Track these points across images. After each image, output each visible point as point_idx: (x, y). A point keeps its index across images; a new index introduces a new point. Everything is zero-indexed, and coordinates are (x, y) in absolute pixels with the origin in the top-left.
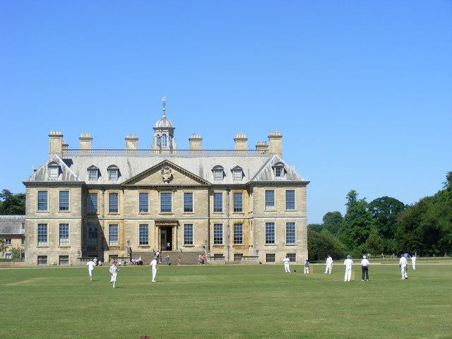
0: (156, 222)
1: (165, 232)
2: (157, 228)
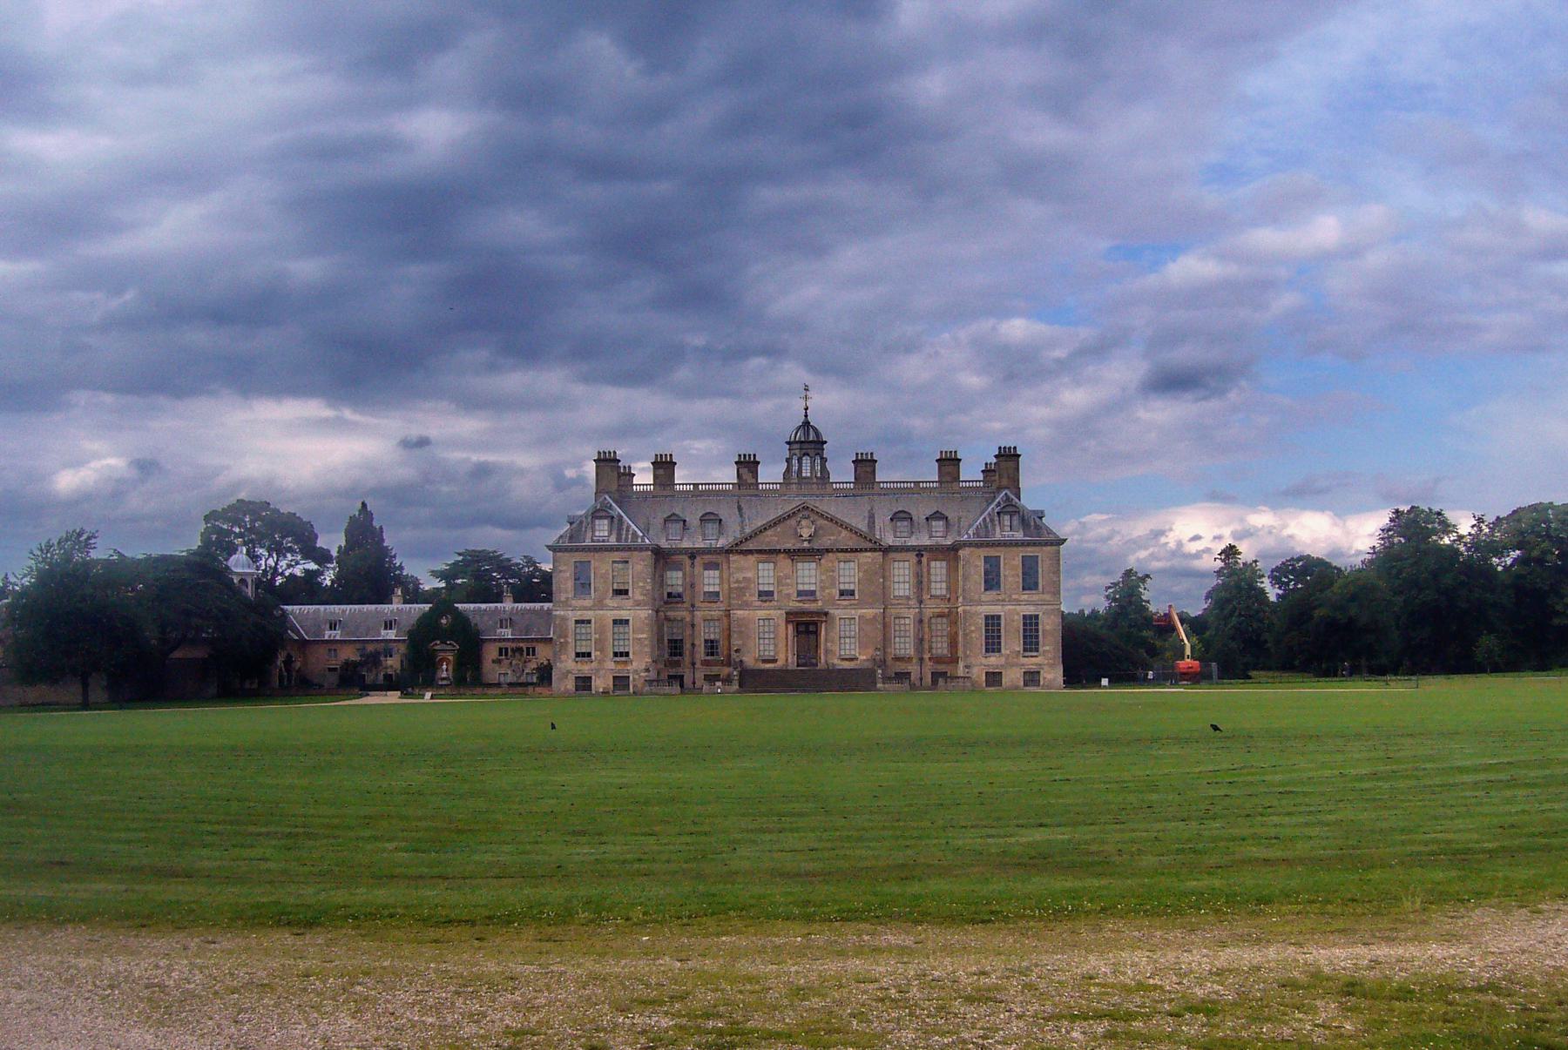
0: (787, 613)
2: (790, 627)
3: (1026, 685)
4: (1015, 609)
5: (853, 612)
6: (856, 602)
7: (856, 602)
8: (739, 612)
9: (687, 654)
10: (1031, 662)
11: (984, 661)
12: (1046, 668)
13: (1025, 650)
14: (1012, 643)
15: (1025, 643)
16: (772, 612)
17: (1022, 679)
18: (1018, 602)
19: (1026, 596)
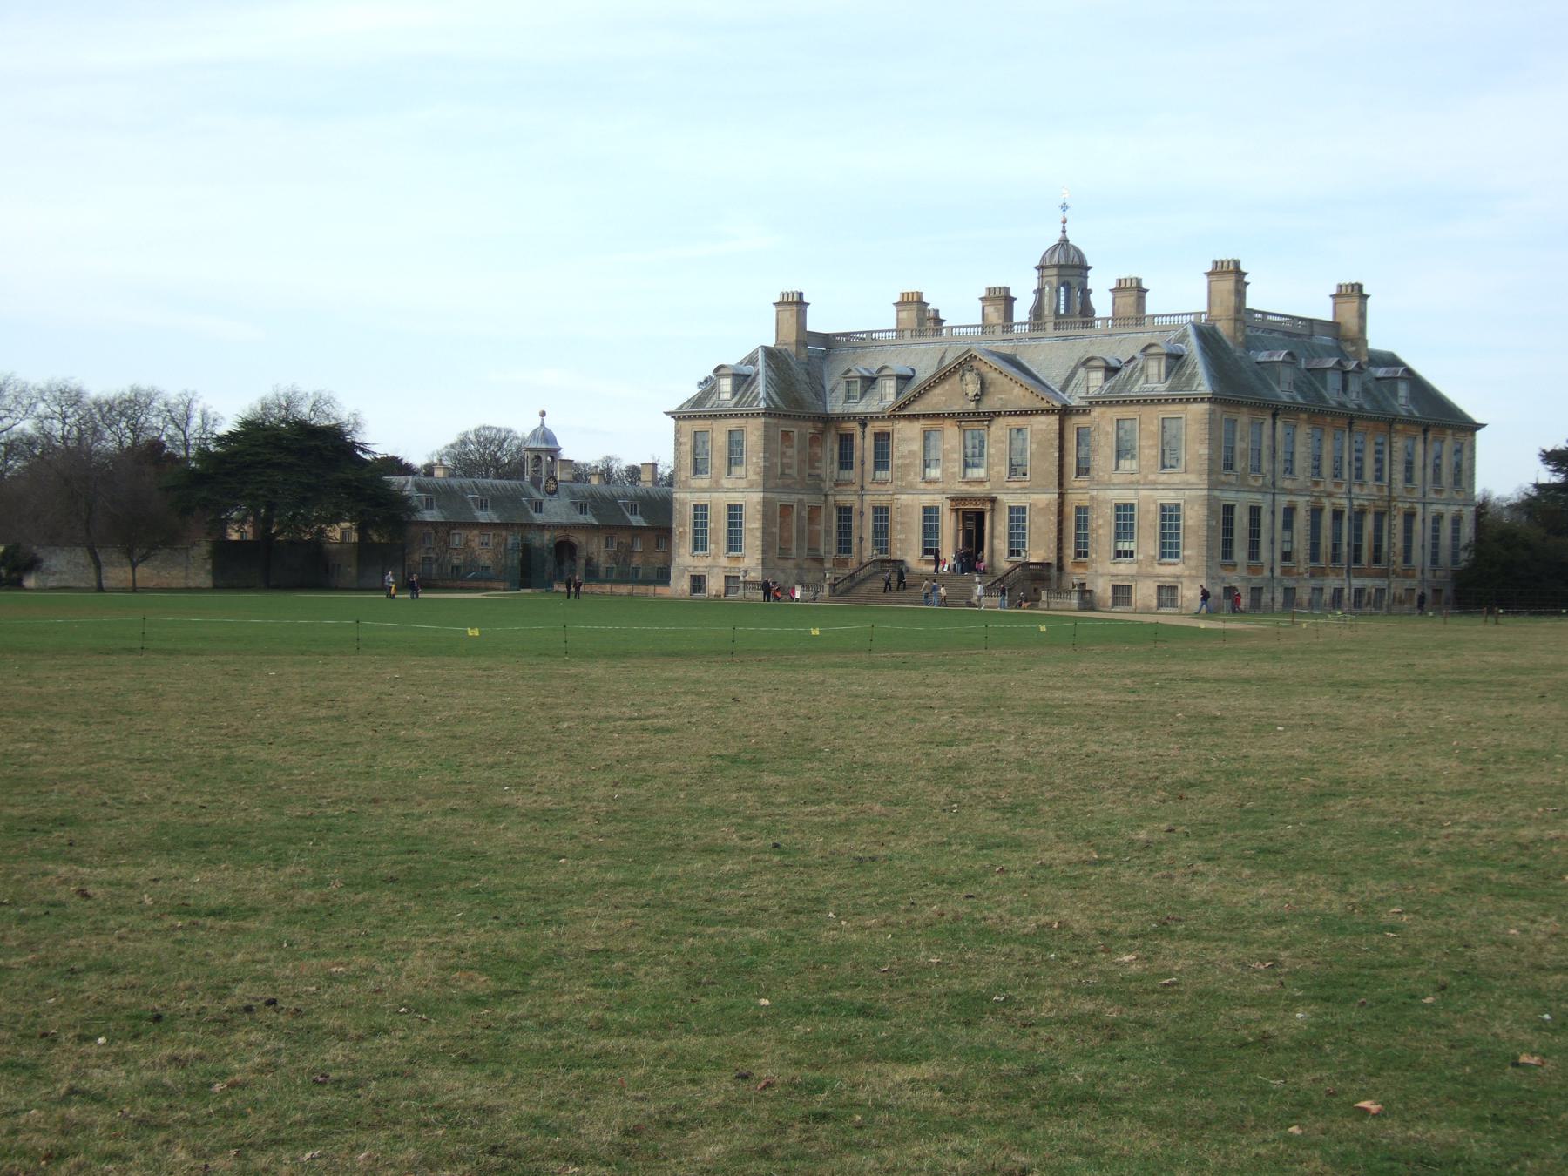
1: (971, 525)
3: (1160, 605)
4: (1151, 496)
5: (1023, 497)
6: (1027, 484)
7: (1027, 484)
8: (904, 497)
9: (855, 549)
10: (1168, 571)
11: (1113, 569)
12: (1186, 582)
13: (1163, 555)
14: (1146, 543)
15: (1163, 545)
16: (937, 497)
17: (1155, 597)
18: (1154, 485)
19: (1165, 477)
